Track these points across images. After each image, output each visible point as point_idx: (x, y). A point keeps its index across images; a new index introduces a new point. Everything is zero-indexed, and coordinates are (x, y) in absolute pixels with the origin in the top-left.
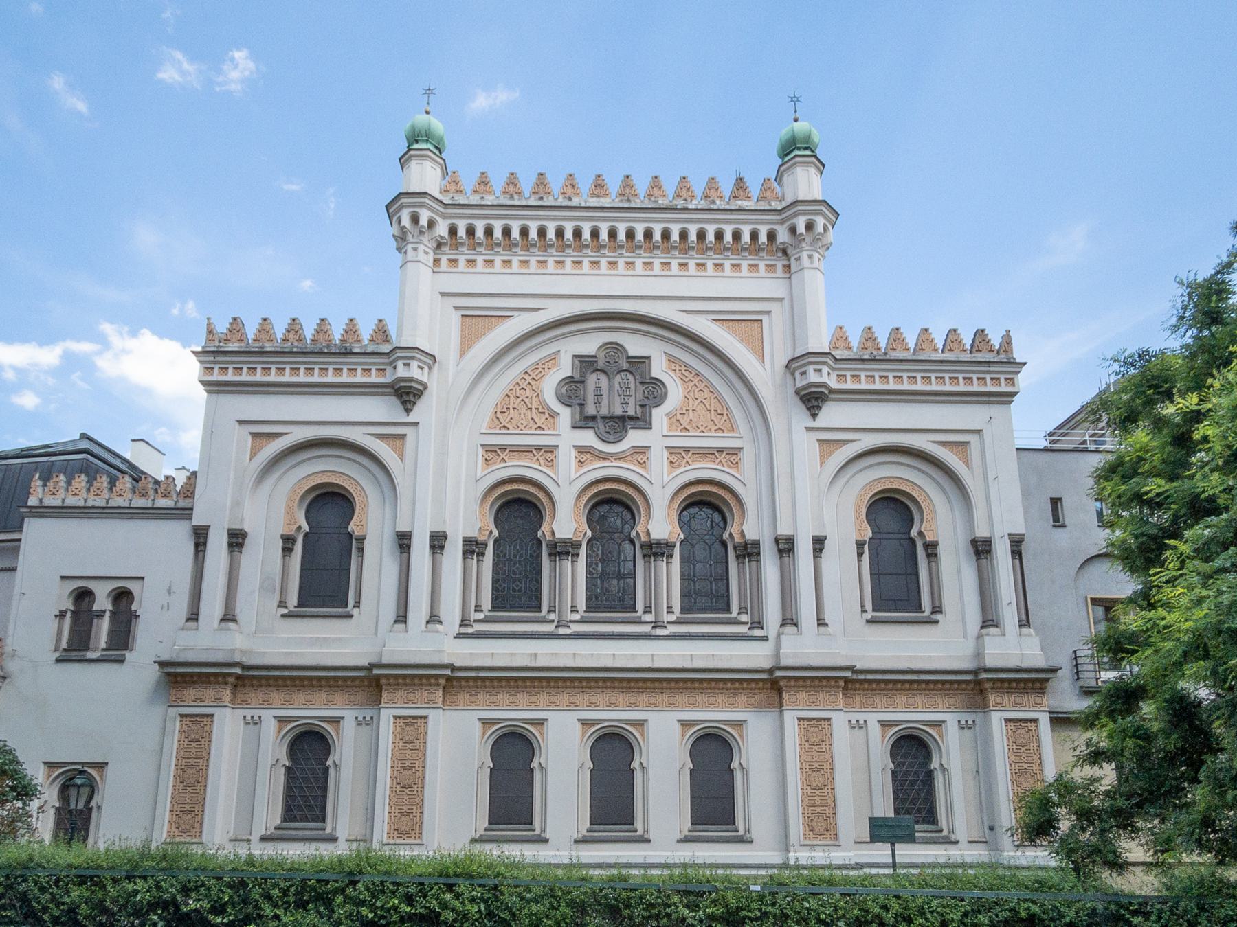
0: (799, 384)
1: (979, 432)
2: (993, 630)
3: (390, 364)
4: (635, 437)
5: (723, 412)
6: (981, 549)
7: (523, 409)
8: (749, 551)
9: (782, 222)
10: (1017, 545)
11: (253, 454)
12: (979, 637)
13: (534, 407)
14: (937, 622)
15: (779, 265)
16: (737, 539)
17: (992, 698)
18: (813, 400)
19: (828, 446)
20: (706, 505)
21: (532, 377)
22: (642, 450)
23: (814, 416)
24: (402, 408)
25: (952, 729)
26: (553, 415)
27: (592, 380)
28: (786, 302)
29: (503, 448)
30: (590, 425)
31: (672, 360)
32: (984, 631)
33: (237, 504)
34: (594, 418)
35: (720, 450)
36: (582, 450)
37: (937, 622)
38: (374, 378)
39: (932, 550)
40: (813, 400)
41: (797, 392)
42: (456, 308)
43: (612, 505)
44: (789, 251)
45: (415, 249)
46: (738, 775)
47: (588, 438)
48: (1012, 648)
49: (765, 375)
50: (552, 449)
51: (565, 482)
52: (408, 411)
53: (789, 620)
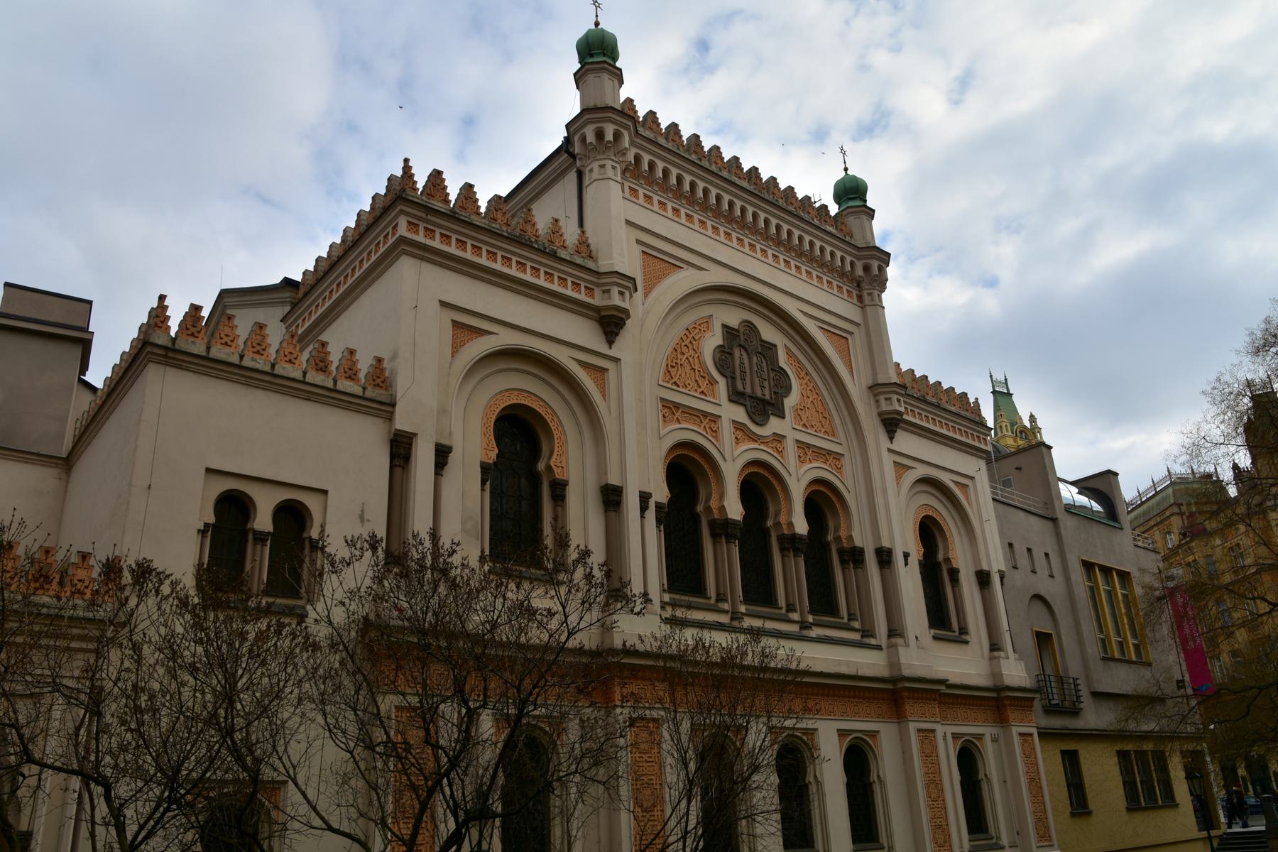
0: (885, 407)
1: (972, 478)
2: (1002, 654)
3: (598, 285)
4: (775, 425)
5: (826, 417)
6: (983, 579)
7: (688, 369)
8: (854, 556)
9: (859, 258)
11: (455, 350)
12: (991, 659)
13: (697, 367)
14: (967, 642)
15: (855, 293)
16: (845, 544)
17: (1012, 714)
18: (891, 424)
19: (901, 468)
20: (822, 502)
21: (690, 339)
22: (779, 438)
23: (891, 439)
24: (603, 337)
25: (988, 739)
26: (713, 382)
27: (737, 352)
28: (862, 327)
29: (677, 406)
30: (742, 401)
31: (790, 354)
32: (996, 653)
33: (443, 411)
34: (742, 394)
35: (830, 452)
36: (738, 426)
37: (967, 642)
38: (582, 297)
39: (954, 574)
40: (891, 424)
41: (880, 414)
42: (638, 242)
43: (760, 486)
44: (863, 285)
45: (602, 166)
46: (877, 788)
47: (739, 414)
48: (1016, 671)
49: (856, 389)
50: (715, 418)
51: (732, 461)
52: (610, 343)
53: (895, 632)
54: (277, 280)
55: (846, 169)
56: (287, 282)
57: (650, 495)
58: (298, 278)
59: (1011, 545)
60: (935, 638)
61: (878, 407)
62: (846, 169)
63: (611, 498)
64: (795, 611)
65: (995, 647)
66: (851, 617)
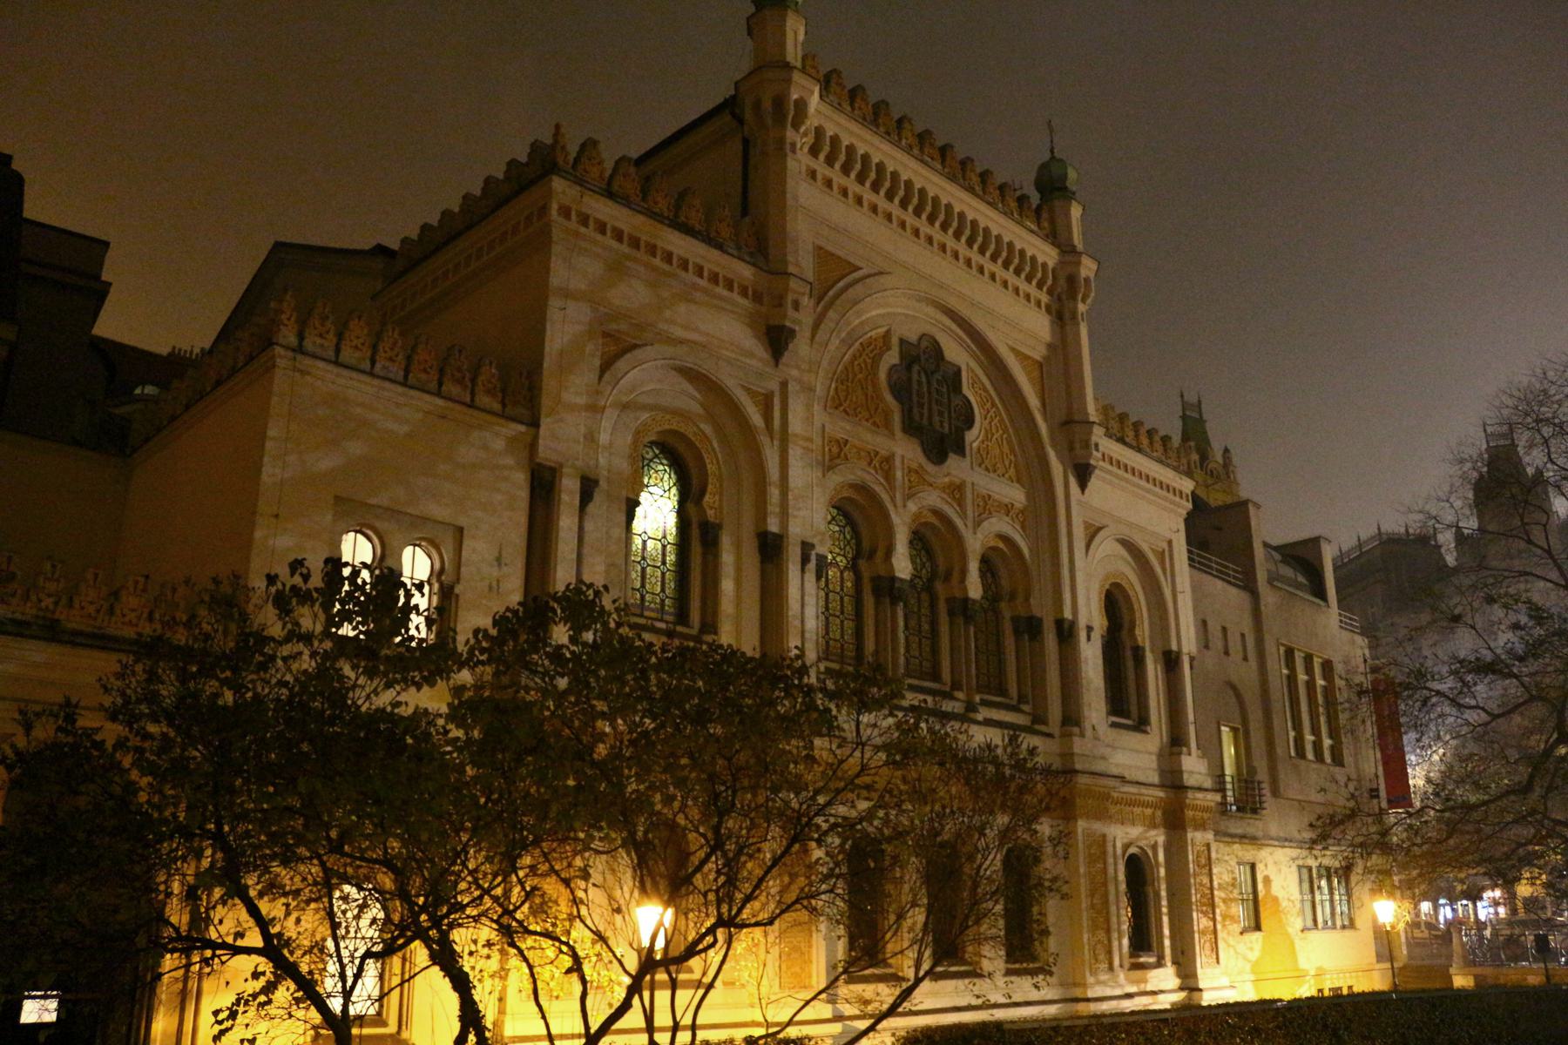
4: (956, 468)
8: (1030, 628)
10: (1192, 659)
14: (1145, 732)
32: (1175, 749)
43: (932, 541)
53: (1072, 719)
54: (366, 244)
55: (1052, 151)
56: (381, 250)
57: (813, 546)
58: (395, 246)
59: (1204, 623)
60: (1114, 725)
61: (1071, 449)
62: (1052, 151)
63: (770, 548)
64: (960, 689)
65: (1177, 741)
66: (1022, 698)
